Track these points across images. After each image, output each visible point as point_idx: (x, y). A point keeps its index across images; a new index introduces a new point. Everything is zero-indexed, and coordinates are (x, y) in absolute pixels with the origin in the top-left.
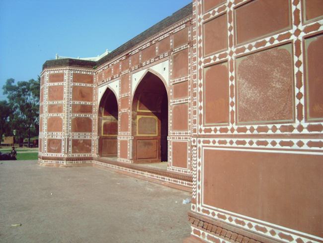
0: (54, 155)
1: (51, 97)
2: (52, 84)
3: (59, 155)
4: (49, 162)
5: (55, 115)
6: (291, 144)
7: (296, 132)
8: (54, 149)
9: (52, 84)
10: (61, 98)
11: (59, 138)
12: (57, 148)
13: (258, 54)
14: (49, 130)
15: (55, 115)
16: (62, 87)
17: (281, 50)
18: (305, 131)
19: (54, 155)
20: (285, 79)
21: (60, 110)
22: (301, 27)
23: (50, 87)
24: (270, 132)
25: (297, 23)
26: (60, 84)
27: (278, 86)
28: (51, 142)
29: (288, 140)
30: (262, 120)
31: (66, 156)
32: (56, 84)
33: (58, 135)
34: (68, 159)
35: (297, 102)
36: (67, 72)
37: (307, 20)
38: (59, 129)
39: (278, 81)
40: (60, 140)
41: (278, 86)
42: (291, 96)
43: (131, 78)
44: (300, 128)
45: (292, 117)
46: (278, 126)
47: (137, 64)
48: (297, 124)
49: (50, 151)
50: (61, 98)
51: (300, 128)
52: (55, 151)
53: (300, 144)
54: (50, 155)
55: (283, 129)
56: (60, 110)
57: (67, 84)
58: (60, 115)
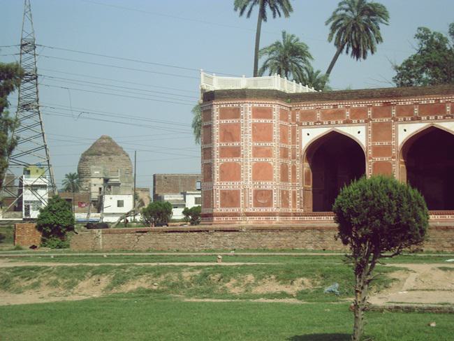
0: (263, 210)
1: (256, 137)
2: (256, 121)
3: (269, 210)
4: (256, 218)
5: (263, 160)
8: (263, 202)
9: (256, 121)
10: (270, 139)
11: (269, 188)
12: (266, 201)
14: (255, 179)
15: (263, 160)
16: (270, 126)
19: (263, 210)
21: (268, 153)
23: (254, 125)
26: (268, 121)
28: (258, 194)
31: (279, 211)
32: (262, 121)
33: (267, 185)
34: (282, 215)
36: (276, 107)
38: (270, 178)
40: (270, 192)
43: (397, 128)
47: (409, 116)
49: (257, 204)
50: (270, 139)
52: (264, 205)
54: (257, 210)
56: (268, 153)
57: (276, 121)
58: (269, 160)
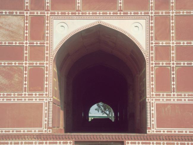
6: (21, 100)
7: (23, 96)
13: (8, 67)
17: (19, 68)
18: (27, 96)
20: (20, 78)
22: (27, 62)
24: (12, 96)
25: (26, 60)
27: (17, 80)
29: (20, 98)
30: (9, 91)
35: (24, 86)
37: (30, 60)
39: (17, 78)
41: (17, 80)
42: (22, 84)
44: (25, 95)
45: (22, 91)
46: (16, 94)
48: (24, 93)
51: (25, 95)
53: (25, 100)
55: (18, 95)
